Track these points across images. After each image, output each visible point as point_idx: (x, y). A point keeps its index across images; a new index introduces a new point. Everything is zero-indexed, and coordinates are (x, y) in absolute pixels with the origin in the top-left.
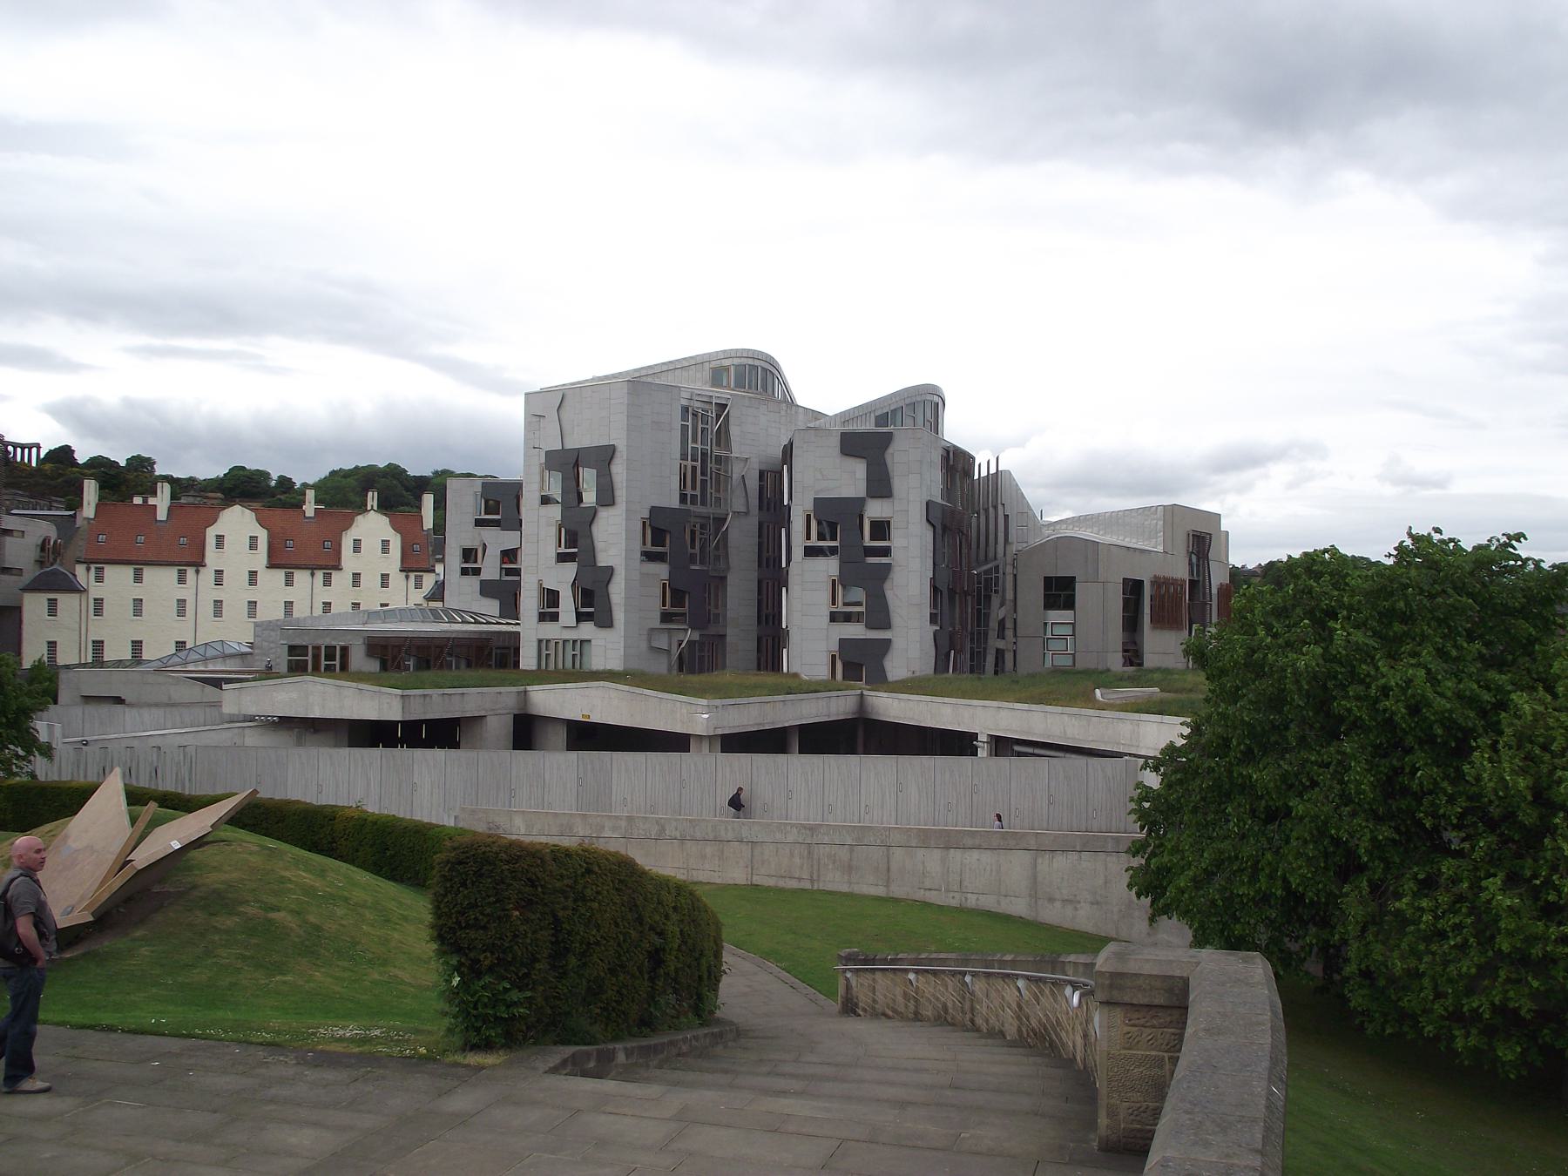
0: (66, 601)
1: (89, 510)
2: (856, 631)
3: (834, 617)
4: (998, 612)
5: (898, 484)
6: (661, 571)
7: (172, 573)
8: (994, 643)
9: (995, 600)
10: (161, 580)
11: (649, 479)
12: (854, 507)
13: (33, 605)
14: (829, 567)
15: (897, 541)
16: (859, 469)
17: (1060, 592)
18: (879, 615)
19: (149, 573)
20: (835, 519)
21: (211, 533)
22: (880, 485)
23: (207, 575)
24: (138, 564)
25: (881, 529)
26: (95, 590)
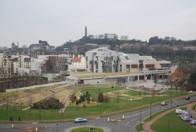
0: (71, 65)
1: (73, 58)
2: (97, 69)
3: (96, 68)
4: (118, 67)
5: (99, 60)
6: (91, 65)
7: (78, 63)
8: (118, 70)
10: (78, 63)
11: (90, 59)
12: (96, 61)
13: (69, 65)
14: (95, 65)
15: (99, 63)
17: (121, 66)
18: (98, 69)
19: (77, 62)
20: (96, 62)
21: (81, 59)
22: (98, 60)
23: (81, 62)
24: (76, 61)
25: (98, 63)
26: (73, 64)
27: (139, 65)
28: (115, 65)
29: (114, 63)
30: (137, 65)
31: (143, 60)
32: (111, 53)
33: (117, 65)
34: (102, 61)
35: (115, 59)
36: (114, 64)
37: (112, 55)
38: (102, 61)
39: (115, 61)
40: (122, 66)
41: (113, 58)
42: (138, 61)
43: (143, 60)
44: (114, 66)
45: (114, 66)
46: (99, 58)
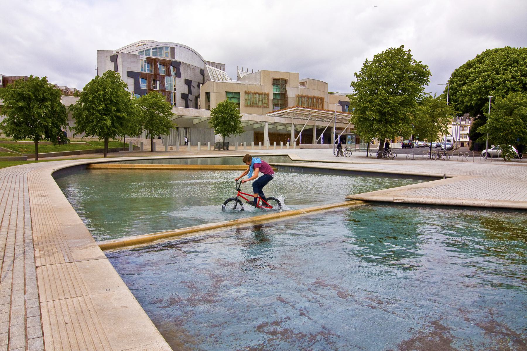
9: (199, 99)
16: (113, 64)
27: (271, 97)
28: (190, 96)
29: (186, 87)
30: (267, 95)
31: (285, 81)
32: (173, 49)
33: (197, 97)
34: (130, 74)
35: (185, 74)
36: (186, 92)
37: (177, 58)
38: (130, 74)
39: (188, 82)
40: (212, 97)
41: (181, 68)
42: (271, 82)
43: (285, 81)
44: (184, 97)
45: (184, 97)
46: (119, 60)
